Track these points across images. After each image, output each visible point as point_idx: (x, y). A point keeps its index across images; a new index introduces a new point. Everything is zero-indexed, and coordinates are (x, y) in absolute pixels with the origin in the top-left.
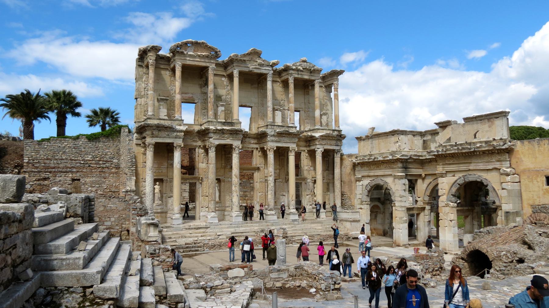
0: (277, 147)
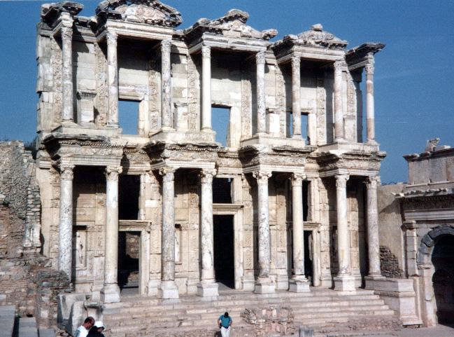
0: (273, 173)
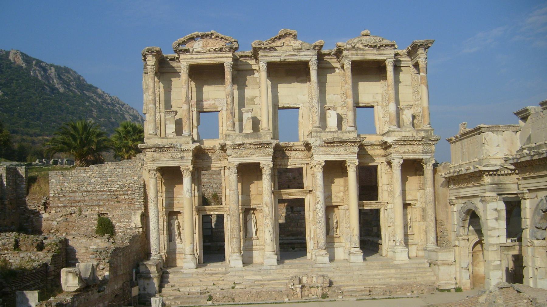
0: (326, 162)
